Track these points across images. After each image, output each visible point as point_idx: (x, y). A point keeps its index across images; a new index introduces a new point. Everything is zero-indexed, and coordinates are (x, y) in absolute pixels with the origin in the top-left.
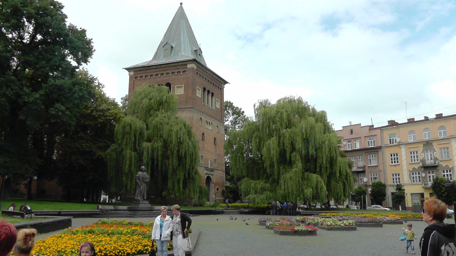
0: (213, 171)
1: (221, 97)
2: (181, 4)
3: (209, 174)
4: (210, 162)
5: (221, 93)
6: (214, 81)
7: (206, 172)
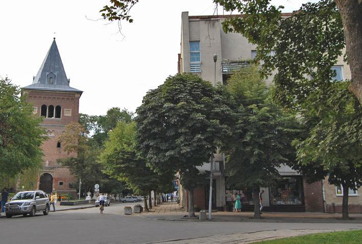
2: (54, 38)
4: (47, 162)
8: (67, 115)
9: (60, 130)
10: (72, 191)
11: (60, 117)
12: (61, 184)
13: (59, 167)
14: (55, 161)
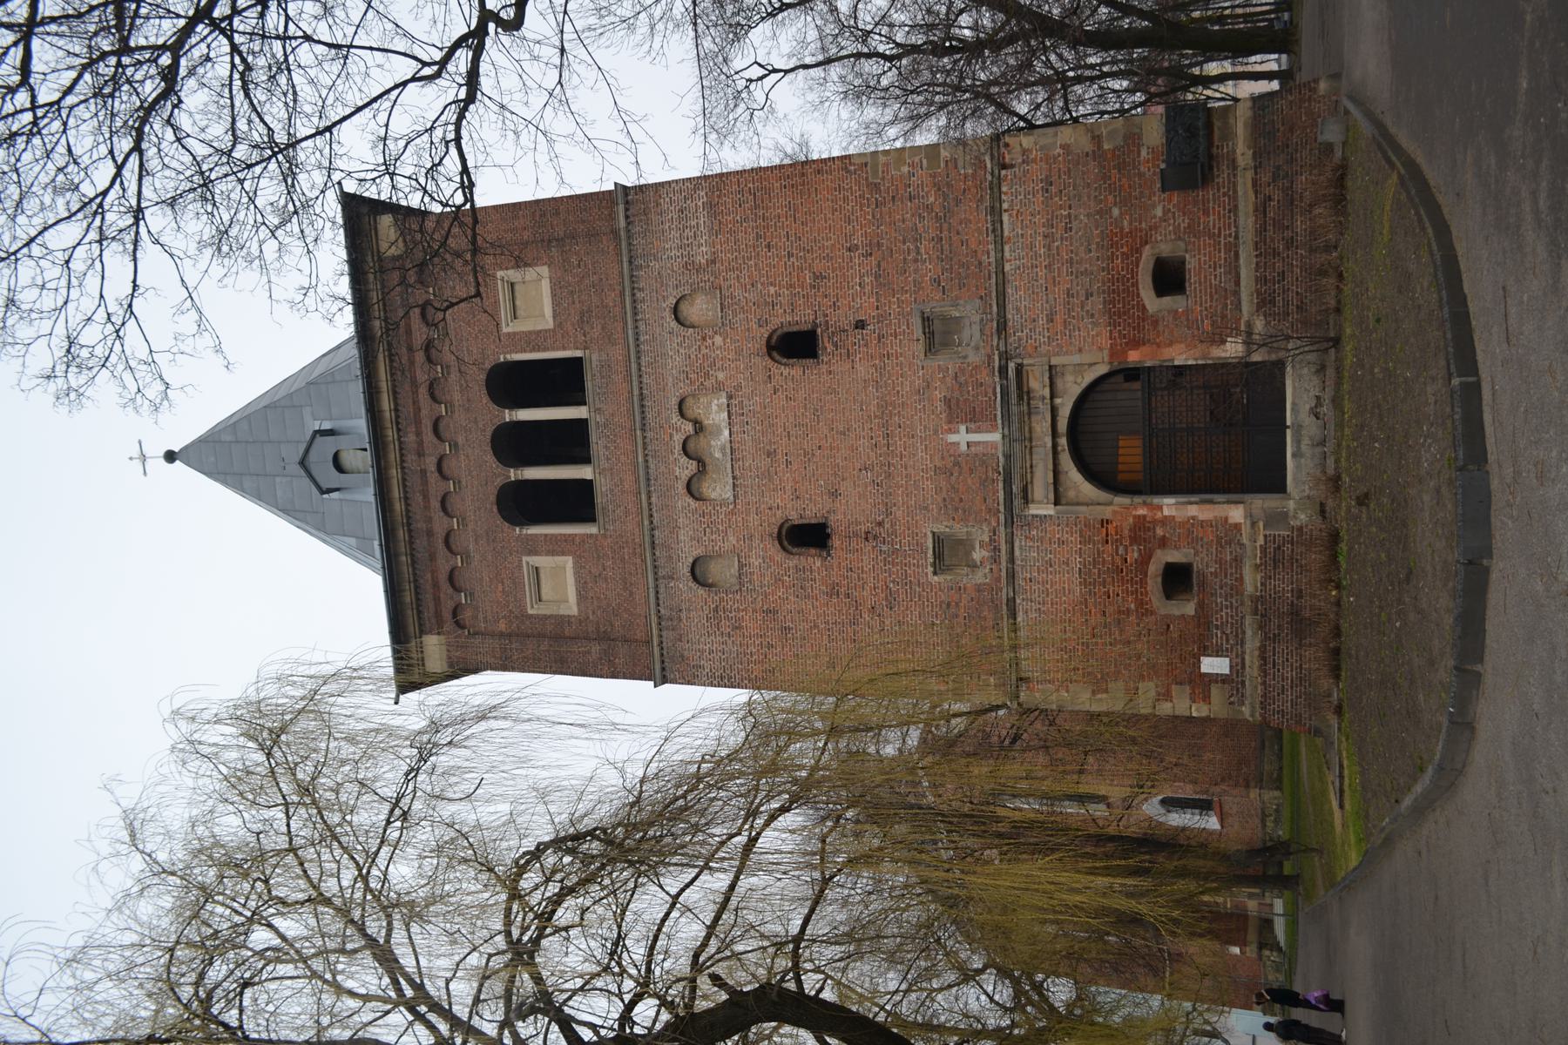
0: (1019, 369)
2: (170, 457)
4: (962, 437)
6: (415, 385)
7: (1042, 508)
8: (548, 311)
10: (1242, 151)
11: (574, 367)
12: (1169, 278)
13: (1002, 327)
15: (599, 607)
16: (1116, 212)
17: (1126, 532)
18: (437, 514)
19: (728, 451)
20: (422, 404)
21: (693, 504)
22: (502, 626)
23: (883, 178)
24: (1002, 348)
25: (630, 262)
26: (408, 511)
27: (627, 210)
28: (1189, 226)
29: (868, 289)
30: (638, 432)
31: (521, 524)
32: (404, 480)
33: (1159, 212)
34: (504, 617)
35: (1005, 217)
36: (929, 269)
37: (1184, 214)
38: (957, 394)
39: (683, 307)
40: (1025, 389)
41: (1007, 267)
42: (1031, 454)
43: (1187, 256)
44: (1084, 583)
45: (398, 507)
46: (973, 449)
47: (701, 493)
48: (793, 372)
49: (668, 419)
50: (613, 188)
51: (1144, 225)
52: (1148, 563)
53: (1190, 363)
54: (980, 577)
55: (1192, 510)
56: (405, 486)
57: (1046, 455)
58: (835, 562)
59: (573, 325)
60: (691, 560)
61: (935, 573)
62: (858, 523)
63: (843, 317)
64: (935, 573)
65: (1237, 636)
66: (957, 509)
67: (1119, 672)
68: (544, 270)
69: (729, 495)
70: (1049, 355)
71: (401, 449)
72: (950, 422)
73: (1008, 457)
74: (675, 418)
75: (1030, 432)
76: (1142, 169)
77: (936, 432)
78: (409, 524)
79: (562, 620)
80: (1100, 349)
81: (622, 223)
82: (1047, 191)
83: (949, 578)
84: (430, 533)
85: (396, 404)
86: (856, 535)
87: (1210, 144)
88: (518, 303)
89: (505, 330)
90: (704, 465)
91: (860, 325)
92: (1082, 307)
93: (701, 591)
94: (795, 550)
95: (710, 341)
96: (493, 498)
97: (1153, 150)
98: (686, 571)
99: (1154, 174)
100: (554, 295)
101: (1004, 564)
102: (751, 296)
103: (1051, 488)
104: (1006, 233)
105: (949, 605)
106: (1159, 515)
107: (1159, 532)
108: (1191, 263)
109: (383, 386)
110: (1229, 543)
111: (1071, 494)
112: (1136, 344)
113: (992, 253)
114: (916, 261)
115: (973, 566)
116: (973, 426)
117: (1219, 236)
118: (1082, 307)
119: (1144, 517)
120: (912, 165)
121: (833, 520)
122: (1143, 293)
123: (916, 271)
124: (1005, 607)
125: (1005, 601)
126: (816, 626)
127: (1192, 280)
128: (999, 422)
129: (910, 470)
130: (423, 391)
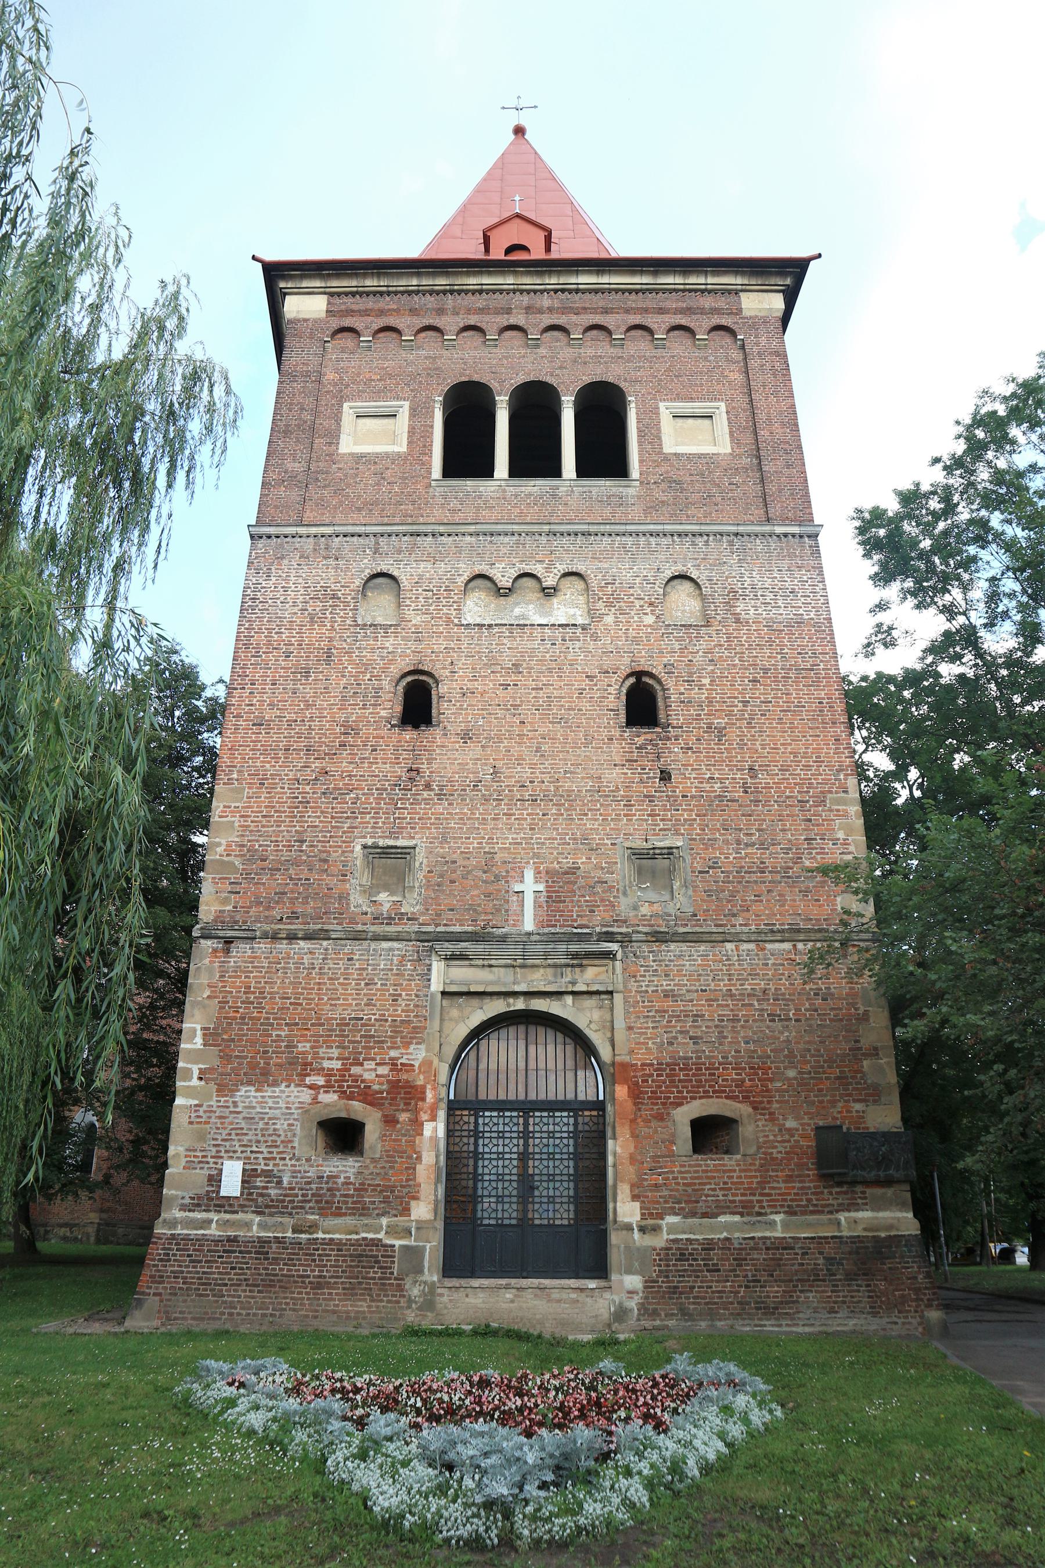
0: (609, 955)
1: (737, 377)
2: (519, 131)
3: (529, 994)
4: (530, 886)
5: (736, 355)
9: (644, 568)
13: (659, 938)
14: (623, 870)
15: (346, 476)
16: (791, 1073)
17: (404, 1076)
18: (462, 321)
19: (521, 622)
20: (582, 316)
21: (461, 580)
22: (330, 376)
23: (831, 810)
24: (635, 937)
25: (736, 534)
26: (467, 292)
27: (793, 536)
28: (773, 1159)
29: (707, 786)
30: (546, 528)
31: (446, 405)
32: (501, 291)
33: (790, 1124)
34: (341, 379)
35: (787, 946)
36: (728, 857)
37: (786, 1153)
38: (581, 882)
39: (687, 586)
40: (585, 962)
41: (729, 946)
42: (506, 966)
43: (739, 1157)
44: (343, 1024)
45: (473, 281)
46: (515, 898)
47: (473, 589)
48: (612, 698)
49: (560, 559)
50: (816, 523)
51: (775, 1105)
52: (364, 1101)
53: (610, 1160)
54: (358, 901)
55: (428, 1158)
56: (494, 291)
57: (505, 984)
58: (384, 732)
59: (667, 472)
60: (395, 573)
61: (365, 847)
62: (430, 761)
63: (675, 755)
64: (365, 847)
65: (267, 1206)
66: (441, 876)
67: (229, 1062)
68: (729, 450)
69: (469, 618)
70: (626, 990)
71: (535, 291)
72: (547, 872)
73: (503, 939)
74: (562, 568)
75: (533, 966)
76: (840, 1104)
77: (536, 855)
78: (452, 292)
79: (334, 436)
80: (631, 1052)
81: (779, 530)
82: (816, 994)
83: (358, 863)
84: (441, 311)
85: (584, 291)
86: (416, 758)
87: (867, 1183)
88: (690, 421)
89: (662, 405)
90: (505, 595)
91: (665, 776)
92: (681, 1032)
93: (358, 582)
94: (400, 689)
95: (648, 610)
96: (476, 378)
97: (861, 1117)
98: (383, 567)
99: (835, 1119)
100: (700, 456)
101: (373, 928)
102: (699, 658)
103: (464, 989)
104: (769, 946)
105: (325, 861)
106: (424, 1116)
107: (404, 1117)
108: (730, 1161)
109: (605, 279)
110: (386, 1201)
111: (455, 1013)
112: (636, 1094)
113: (746, 929)
114: (739, 842)
115: (370, 891)
116: (542, 899)
117: (761, 1195)
118: (681, 1032)
119: (423, 1099)
120: (845, 843)
121: (438, 732)
122: (697, 1103)
123: (727, 842)
124: (319, 926)
125: (326, 927)
126: (308, 706)
127: (709, 1162)
128: (546, 930)
129: (491, 824)
130: (598, 319)
